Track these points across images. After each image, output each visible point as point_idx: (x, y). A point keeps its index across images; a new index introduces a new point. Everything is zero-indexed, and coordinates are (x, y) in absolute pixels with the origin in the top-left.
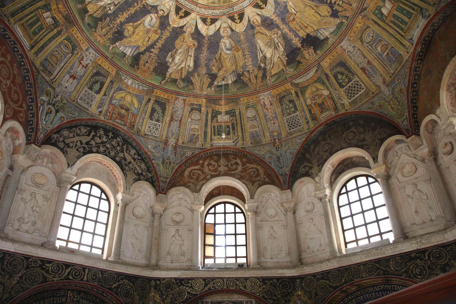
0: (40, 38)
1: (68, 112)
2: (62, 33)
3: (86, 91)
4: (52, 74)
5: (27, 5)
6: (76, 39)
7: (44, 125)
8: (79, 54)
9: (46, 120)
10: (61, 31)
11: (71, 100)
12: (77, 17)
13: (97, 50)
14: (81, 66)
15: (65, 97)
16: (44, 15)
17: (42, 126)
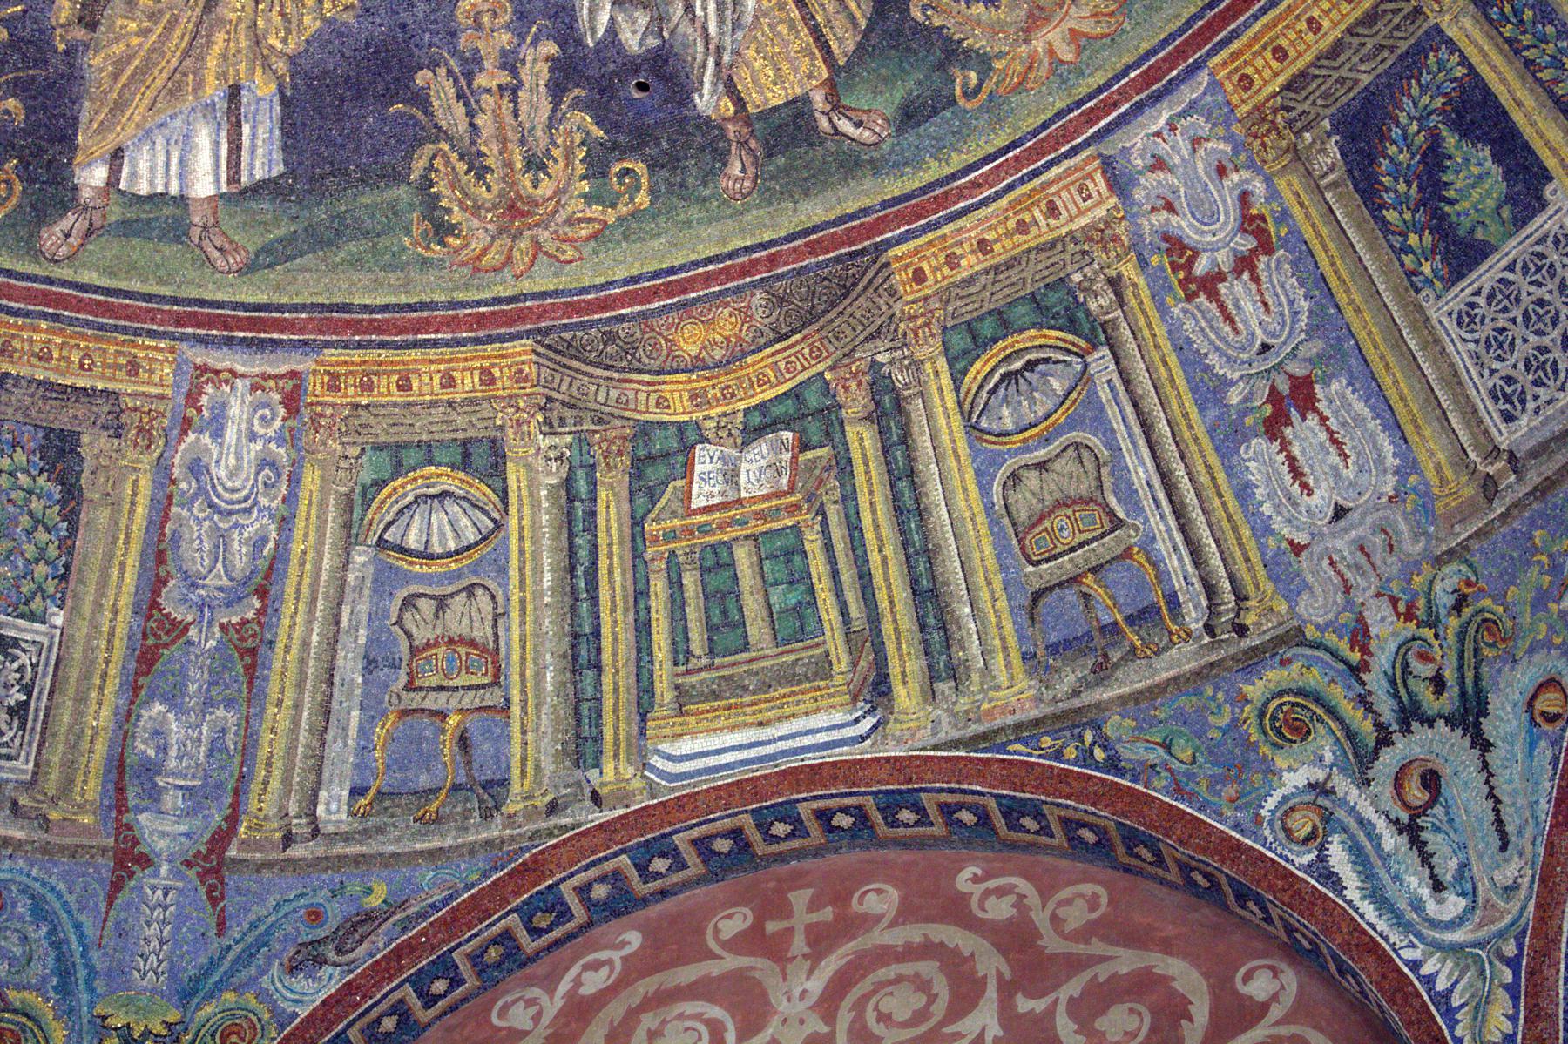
0: (851, 596)
1: (1541, 601)
2: (900, 378)
3: (1466, 319)
4: (1173, 601)
5: (573, 609)
6: (996, 269)
7: (1452, 925)
8: (1129, 270)
9: (1447, 873)
10: (880, 385)
11: (1464, 513)
12: (814, 211)
13: (1148, 79)
14: (1236, 290)
15: (1410, 568)
16: (698, 502)
17: (1456, 949)
